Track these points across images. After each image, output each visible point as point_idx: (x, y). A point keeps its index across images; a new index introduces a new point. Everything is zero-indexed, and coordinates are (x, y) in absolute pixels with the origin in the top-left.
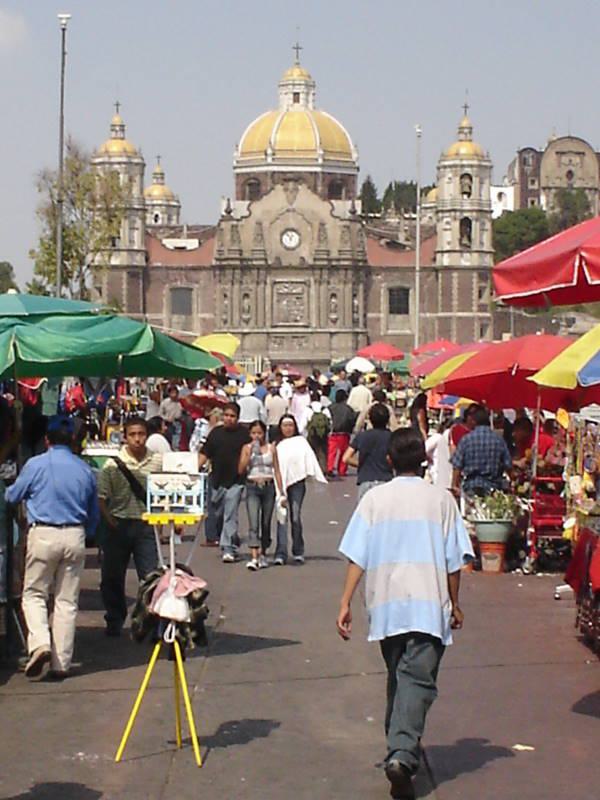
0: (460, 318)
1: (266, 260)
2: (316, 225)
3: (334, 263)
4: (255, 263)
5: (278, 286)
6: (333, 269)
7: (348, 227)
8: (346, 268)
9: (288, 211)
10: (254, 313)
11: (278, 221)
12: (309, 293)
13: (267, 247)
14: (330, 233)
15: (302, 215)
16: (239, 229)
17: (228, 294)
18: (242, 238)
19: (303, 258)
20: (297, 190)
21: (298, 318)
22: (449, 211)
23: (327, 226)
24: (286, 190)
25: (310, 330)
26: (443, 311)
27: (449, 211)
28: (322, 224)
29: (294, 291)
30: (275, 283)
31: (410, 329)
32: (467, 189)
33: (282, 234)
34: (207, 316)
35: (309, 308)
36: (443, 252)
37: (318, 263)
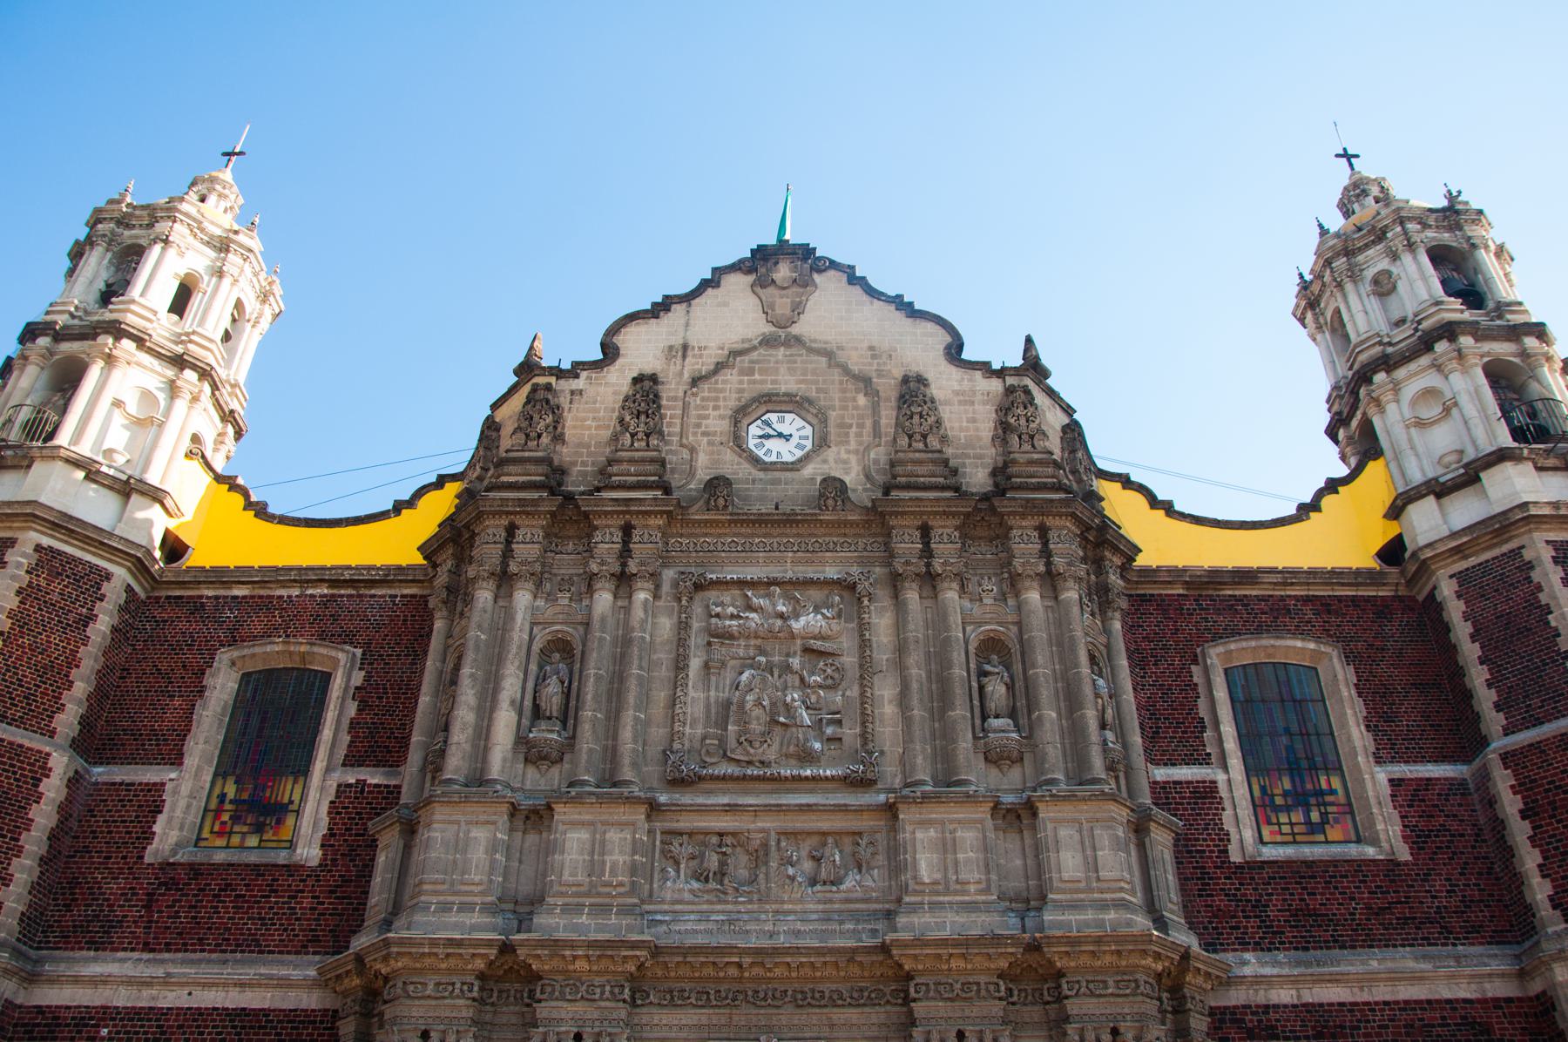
2: (888, 388)
9: (768, 342)
11: (730, 378)
12: (863, 627)
14: (945, 413)
15: (829, 354)
16: (564, 401)
18: (569, 433)
19: (833, 489)
20: (803, 283)
21: (817, 746)
22: (1426, 343)
23: (935, 391)
24: (763, 283)
26: (1507, 732)
29: (797, 625)
31: (1375, 842)
33: (740, 416)
34: (374, 777)
36: (1439, 490)
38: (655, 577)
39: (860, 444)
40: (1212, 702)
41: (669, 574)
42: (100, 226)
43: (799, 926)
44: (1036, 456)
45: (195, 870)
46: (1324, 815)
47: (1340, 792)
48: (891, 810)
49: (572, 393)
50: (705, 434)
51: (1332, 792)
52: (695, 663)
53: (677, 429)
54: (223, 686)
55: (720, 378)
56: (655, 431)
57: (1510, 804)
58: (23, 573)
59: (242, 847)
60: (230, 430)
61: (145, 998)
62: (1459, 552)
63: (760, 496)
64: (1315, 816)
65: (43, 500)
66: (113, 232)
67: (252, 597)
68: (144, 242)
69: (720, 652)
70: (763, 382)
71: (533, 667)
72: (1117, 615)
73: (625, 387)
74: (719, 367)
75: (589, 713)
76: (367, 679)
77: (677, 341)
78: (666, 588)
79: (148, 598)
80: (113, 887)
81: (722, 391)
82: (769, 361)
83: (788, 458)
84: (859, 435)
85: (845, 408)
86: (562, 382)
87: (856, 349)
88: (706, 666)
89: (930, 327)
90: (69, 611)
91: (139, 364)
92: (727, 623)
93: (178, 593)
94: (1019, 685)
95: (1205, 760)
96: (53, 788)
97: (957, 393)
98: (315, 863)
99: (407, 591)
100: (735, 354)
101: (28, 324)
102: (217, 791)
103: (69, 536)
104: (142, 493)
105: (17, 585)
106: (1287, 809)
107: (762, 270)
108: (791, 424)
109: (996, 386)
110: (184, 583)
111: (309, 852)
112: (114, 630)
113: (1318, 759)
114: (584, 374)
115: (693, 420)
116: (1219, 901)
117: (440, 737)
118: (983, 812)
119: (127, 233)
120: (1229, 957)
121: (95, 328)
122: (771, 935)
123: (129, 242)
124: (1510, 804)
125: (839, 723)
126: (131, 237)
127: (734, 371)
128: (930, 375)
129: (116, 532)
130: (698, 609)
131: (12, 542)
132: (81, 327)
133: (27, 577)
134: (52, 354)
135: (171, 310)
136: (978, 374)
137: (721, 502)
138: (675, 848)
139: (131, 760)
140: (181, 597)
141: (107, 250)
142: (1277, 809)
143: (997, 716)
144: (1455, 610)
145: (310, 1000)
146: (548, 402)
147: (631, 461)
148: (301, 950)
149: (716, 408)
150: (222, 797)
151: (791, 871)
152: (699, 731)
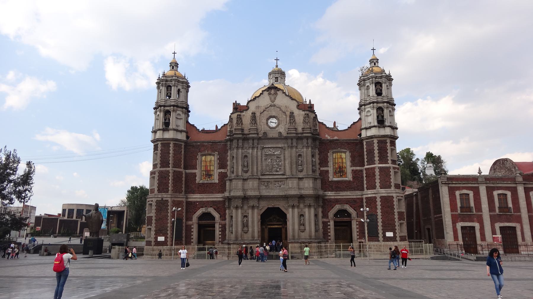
0: (380, 168)
1: (258, 134)
2: (288, 113)
3: (300, 135)
4: (251, 136)
5: (265, 150)
6: (299, 138)
7: (308, 114)
8: (307, 138)
10: (250, 167)
11: (265, 112)
13: (259, 127)
17: (235, 156)
19: (280, 133)
20: (276, 94)
21: (278, 170)
22: (370, 103)
23: (295, 114)
24: (270, 94)
25: (285, 177)
27: (370, 103)
28: (292, 113)
29: (275, 153)
30: (263, 148)
32: (379, 91)
33: (268, 119)
34: (223, 171)
35: (285, 164)
36: (366, 129)
37: (289, 135)
38: (257, 147)
39: (284, 124)
40: (330, 159)
41: (259, 146)
43: (276, 192)
44: (308, 127)
45: (203, 184)
46: (343, 174)
47: (346, 171)
48: (287, 178)
49: (243, 115)
50: (262, 123)
51: (344, 171)
52: (263, 159)
53: (258, 122)
55: (264, 112)
56: (256, 123)
57: (365, 175)
59: (208, 180)
61: (201, 200)
62: (367, 139)
63: (271, 135)
64: (341, 174)
69: (266, 157)
70: (270, 113)
71: (243, 160)
72: (317, 149)
73: (251, 114)
74: (264, 111)
75: (250, 167)
76: (219, 157)
77: (257, 105)
78: (259, 148)
80: (193, 186)
81: (264, 115)
82: (271, 109)
83: (274, 126)
84: (284, 122)
85: (282, 118)
86: (241, 113)
87: (283, 106)
88: (265, 159)
89: (294, 102)
92: (267, 153)
93: (190, 144)
94: (303, 161)
95: (328, 167)
96: (184, 175)
97: (298, 114)
98: (218, 182)
99: (223, 143)
100: (266, 108)
102: (202, 173)
105: (173, 150)
106: (338, 173)
107: (269, 91)
108: (274, 120)
109: (303, 113)
111: (217, 181)
113: (343, 166)
114: (244, 112)
115: (261, 120)
116: (327, 186)
117: (232, 169)
118: (297, 179)
120: (326, 193)
122: (273, 193)
123: (168, 85)
124: (365, 175)
125: (281, 167)
127: (266, 111)
128: (294, 112)
130: (263, 151)
136: (301, 111)
137: (265, 136)
138: (262, 183)
139: (190, 169)
141: (165, 87)
142: (337, 173)
143: (300, 166)
144: (365, 147)
145: (221, 199)
146: (240, 118)
147: (253, 129)
148: (218, 193)
149: (264, 118)
150: (203, 174)
151: (275, 185)
152: (264, 168)
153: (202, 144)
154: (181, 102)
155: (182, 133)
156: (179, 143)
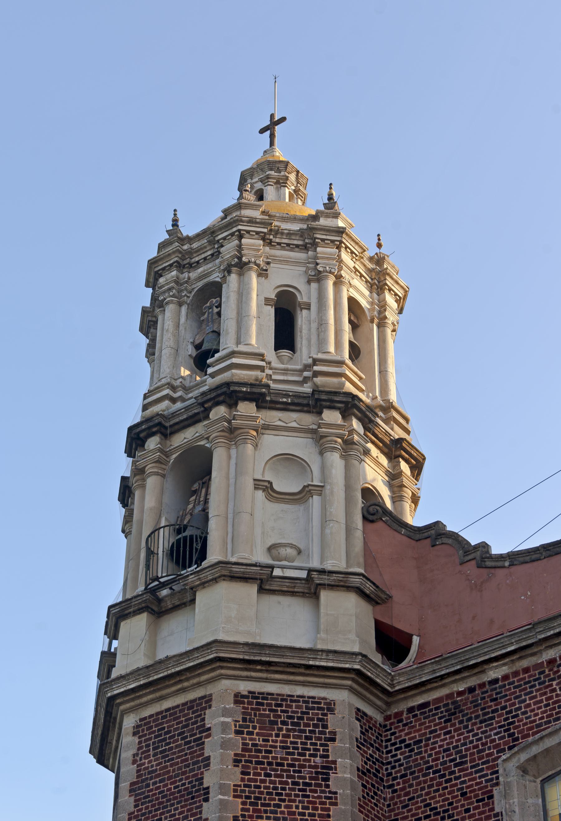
42: (162, 280)
54: (522, 805)
58: (232, 736)
60: (404, 467)
65: (221, 636)
66: (177, 282)
67: (516, 674)
68: (216, 277)
79: (387, 718)
90: (301, 766)
91: (267, 427)
93: (420, 700)
101: (130, 429)
103: (267, 671)
104: (332, 587)
105: (231, 753)
110: (423, 684)
112: (362, 773)
119: (194, 275)
121: (202, 404)
123: (200, 284)
126: (200, 278)
129: (319, 647)
131: (207, 700)
132: (187, 408)
133: (239, 738)
134: (167, 454)
135: (277, 347)
140: (425, 705)
141: (180, 305)
153: (525, 663)
154: (301, 371)
155: (324, 595)
156: (299, 691)
